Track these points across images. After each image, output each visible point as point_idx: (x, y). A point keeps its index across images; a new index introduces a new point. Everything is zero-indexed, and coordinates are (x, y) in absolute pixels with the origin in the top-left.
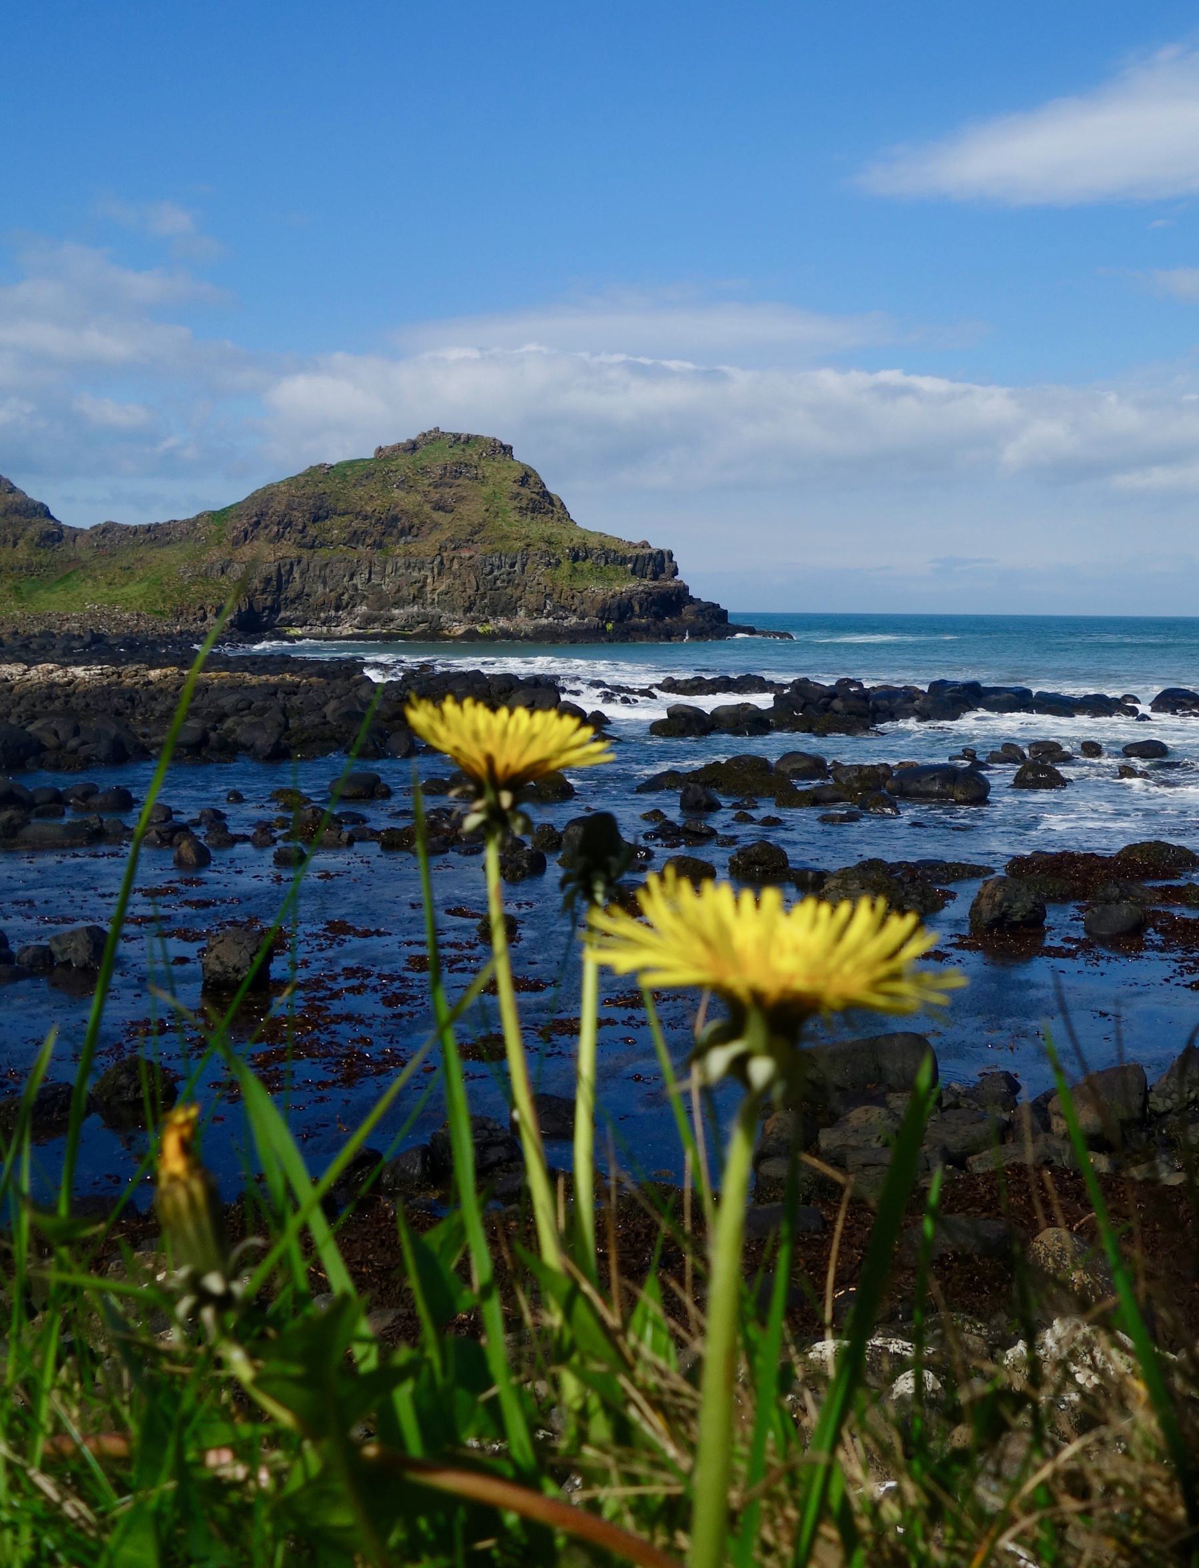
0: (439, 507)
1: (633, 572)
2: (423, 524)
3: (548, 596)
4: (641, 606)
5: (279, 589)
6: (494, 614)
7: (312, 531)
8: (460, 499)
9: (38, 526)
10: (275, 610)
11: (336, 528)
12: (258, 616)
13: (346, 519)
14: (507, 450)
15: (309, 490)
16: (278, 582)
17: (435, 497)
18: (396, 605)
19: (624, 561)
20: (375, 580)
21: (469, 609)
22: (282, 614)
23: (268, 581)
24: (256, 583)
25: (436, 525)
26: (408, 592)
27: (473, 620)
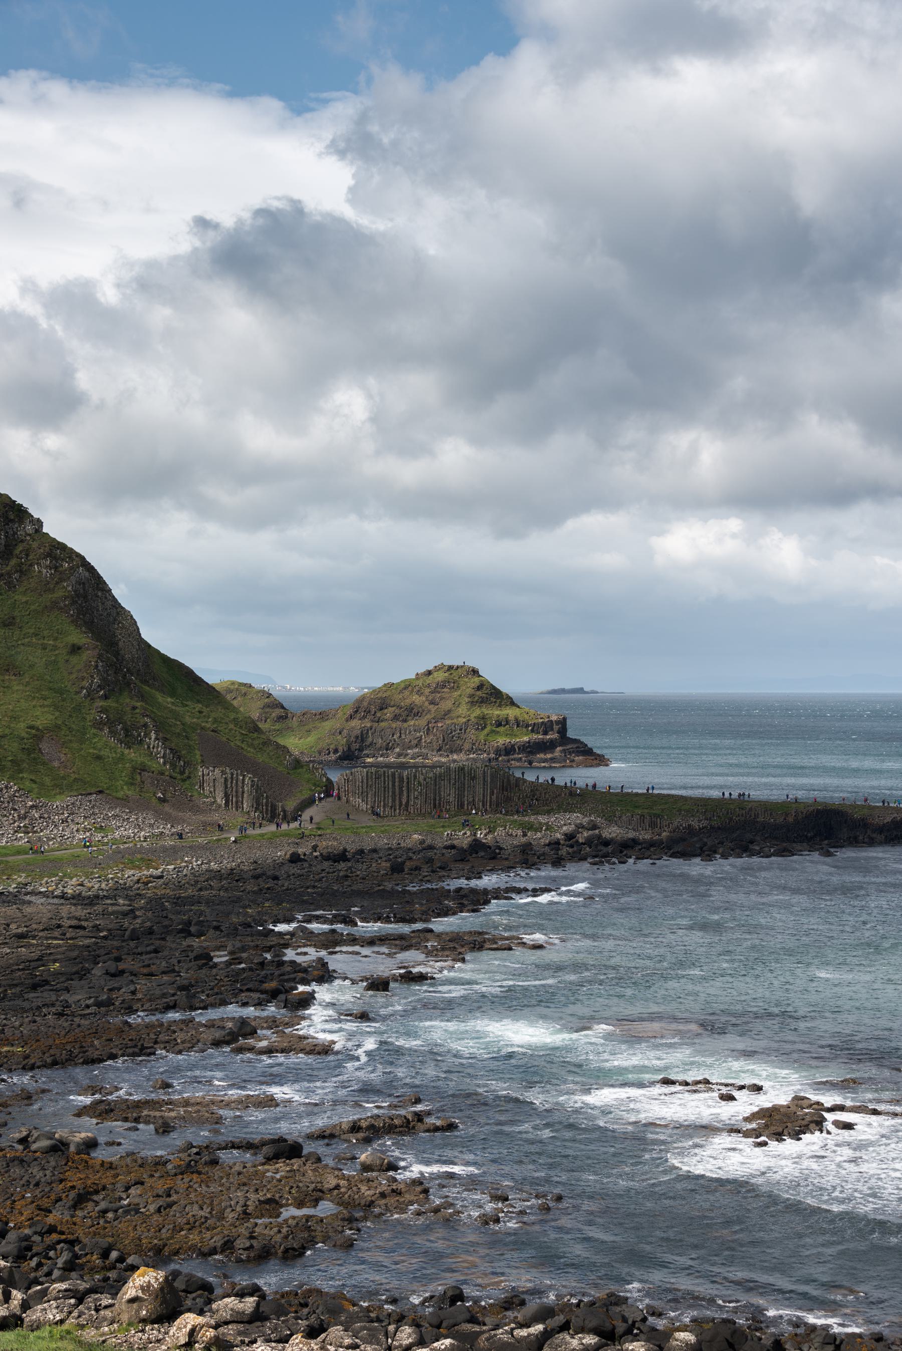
0: (432, 703)
1: (532, 731)
2: (423, 711)
3: (474, 744)
4: (519, 748)
5: (363, 741)
6: (452, 752)
7: (378, 714)
8: (442, 698)
9: (278, 712)
10: (361, 750)
11: (389, 713)
12: (353, 753)
13: (393, 709)
15: (379, 695)
16: (362, 737)
17: (430, 698)
18: (409, 748)
19: (527, 726)
20: (403, 736)
21: (440, 750)
22: (365, 752)
23: (357, 737)
24: (352, 739)
25: (429, 711)
26: (414, 742)
27: (441, 755)
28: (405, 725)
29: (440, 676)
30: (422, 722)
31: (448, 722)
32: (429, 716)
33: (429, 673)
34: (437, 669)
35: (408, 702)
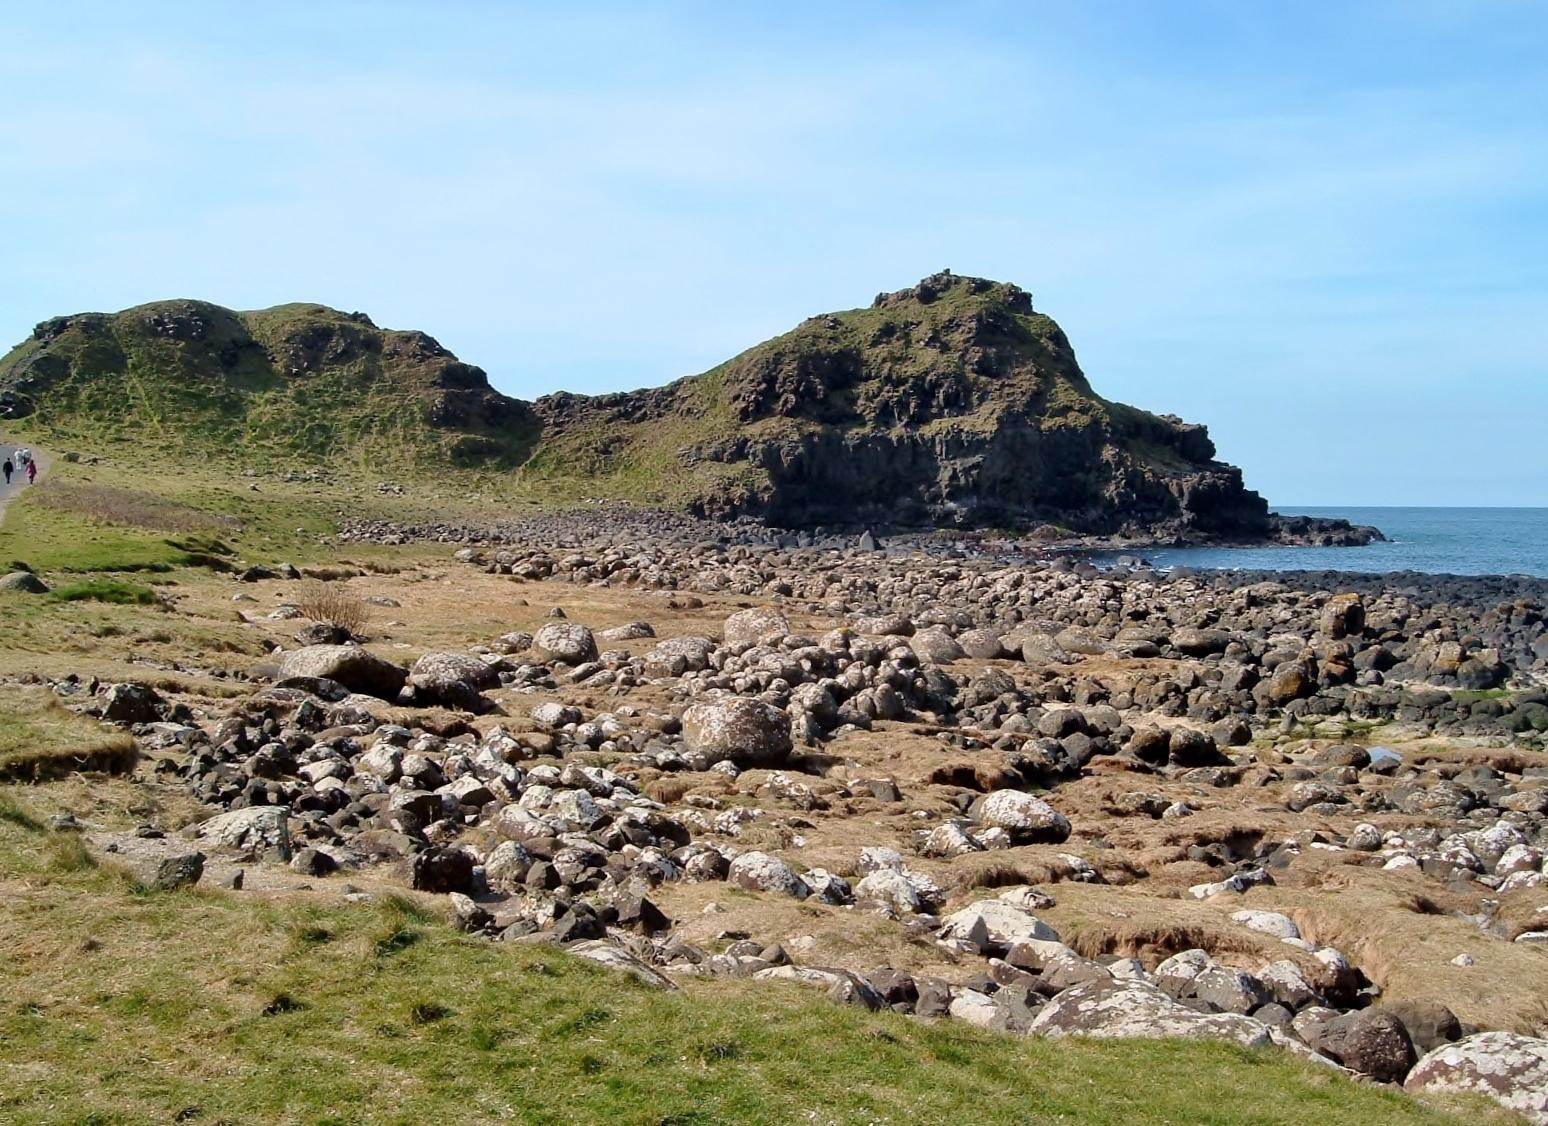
13: (874, 385)
14: (1027, 298)
28: (927, 431)
30: (982, 420)
31: (1047, 424)
35: (910, 370)
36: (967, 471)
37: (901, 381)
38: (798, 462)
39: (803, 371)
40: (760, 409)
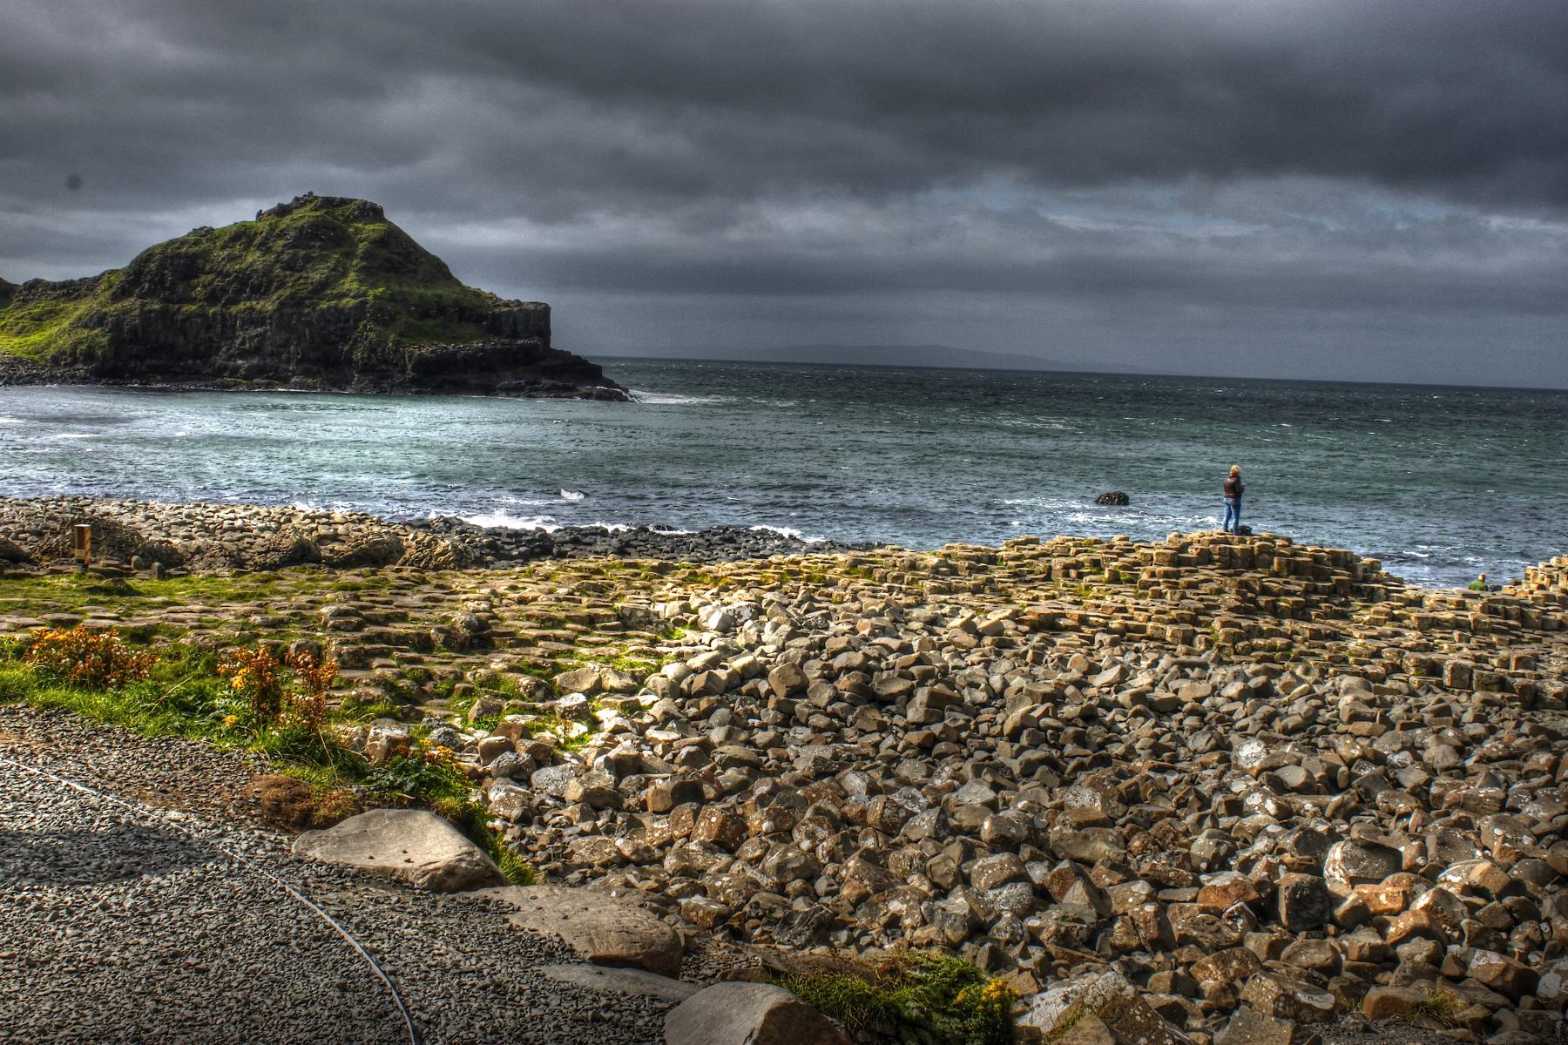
0: (289, 266)
2: (270, 283)
7: (181, 288)
13: (211, 277)
19: (480, 318)
28: (234, 309)
29: (305, 215)
30: (268, 305)
31: (324, 305)
32: (285, 293)
33: (282, 211)
34: (299, 203)
36: (251, 339)
37: (228, 275)
38: (134, 330)
39: (162, 266)
40: (122, 293)
